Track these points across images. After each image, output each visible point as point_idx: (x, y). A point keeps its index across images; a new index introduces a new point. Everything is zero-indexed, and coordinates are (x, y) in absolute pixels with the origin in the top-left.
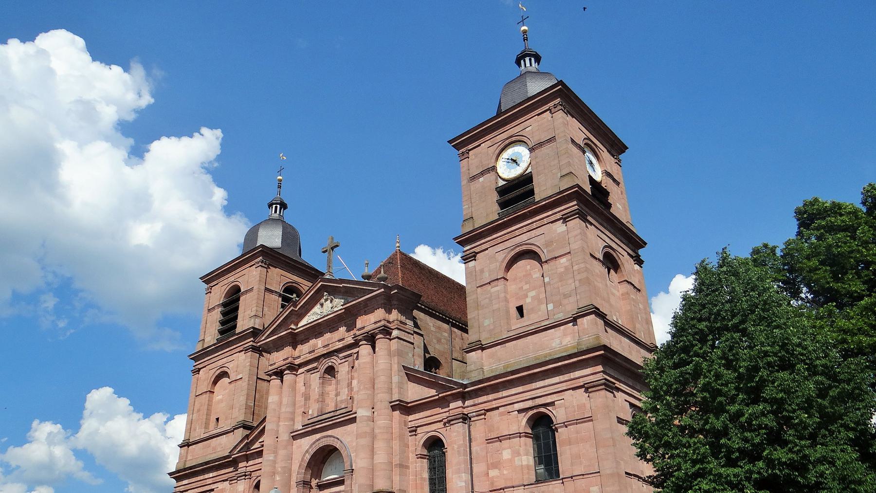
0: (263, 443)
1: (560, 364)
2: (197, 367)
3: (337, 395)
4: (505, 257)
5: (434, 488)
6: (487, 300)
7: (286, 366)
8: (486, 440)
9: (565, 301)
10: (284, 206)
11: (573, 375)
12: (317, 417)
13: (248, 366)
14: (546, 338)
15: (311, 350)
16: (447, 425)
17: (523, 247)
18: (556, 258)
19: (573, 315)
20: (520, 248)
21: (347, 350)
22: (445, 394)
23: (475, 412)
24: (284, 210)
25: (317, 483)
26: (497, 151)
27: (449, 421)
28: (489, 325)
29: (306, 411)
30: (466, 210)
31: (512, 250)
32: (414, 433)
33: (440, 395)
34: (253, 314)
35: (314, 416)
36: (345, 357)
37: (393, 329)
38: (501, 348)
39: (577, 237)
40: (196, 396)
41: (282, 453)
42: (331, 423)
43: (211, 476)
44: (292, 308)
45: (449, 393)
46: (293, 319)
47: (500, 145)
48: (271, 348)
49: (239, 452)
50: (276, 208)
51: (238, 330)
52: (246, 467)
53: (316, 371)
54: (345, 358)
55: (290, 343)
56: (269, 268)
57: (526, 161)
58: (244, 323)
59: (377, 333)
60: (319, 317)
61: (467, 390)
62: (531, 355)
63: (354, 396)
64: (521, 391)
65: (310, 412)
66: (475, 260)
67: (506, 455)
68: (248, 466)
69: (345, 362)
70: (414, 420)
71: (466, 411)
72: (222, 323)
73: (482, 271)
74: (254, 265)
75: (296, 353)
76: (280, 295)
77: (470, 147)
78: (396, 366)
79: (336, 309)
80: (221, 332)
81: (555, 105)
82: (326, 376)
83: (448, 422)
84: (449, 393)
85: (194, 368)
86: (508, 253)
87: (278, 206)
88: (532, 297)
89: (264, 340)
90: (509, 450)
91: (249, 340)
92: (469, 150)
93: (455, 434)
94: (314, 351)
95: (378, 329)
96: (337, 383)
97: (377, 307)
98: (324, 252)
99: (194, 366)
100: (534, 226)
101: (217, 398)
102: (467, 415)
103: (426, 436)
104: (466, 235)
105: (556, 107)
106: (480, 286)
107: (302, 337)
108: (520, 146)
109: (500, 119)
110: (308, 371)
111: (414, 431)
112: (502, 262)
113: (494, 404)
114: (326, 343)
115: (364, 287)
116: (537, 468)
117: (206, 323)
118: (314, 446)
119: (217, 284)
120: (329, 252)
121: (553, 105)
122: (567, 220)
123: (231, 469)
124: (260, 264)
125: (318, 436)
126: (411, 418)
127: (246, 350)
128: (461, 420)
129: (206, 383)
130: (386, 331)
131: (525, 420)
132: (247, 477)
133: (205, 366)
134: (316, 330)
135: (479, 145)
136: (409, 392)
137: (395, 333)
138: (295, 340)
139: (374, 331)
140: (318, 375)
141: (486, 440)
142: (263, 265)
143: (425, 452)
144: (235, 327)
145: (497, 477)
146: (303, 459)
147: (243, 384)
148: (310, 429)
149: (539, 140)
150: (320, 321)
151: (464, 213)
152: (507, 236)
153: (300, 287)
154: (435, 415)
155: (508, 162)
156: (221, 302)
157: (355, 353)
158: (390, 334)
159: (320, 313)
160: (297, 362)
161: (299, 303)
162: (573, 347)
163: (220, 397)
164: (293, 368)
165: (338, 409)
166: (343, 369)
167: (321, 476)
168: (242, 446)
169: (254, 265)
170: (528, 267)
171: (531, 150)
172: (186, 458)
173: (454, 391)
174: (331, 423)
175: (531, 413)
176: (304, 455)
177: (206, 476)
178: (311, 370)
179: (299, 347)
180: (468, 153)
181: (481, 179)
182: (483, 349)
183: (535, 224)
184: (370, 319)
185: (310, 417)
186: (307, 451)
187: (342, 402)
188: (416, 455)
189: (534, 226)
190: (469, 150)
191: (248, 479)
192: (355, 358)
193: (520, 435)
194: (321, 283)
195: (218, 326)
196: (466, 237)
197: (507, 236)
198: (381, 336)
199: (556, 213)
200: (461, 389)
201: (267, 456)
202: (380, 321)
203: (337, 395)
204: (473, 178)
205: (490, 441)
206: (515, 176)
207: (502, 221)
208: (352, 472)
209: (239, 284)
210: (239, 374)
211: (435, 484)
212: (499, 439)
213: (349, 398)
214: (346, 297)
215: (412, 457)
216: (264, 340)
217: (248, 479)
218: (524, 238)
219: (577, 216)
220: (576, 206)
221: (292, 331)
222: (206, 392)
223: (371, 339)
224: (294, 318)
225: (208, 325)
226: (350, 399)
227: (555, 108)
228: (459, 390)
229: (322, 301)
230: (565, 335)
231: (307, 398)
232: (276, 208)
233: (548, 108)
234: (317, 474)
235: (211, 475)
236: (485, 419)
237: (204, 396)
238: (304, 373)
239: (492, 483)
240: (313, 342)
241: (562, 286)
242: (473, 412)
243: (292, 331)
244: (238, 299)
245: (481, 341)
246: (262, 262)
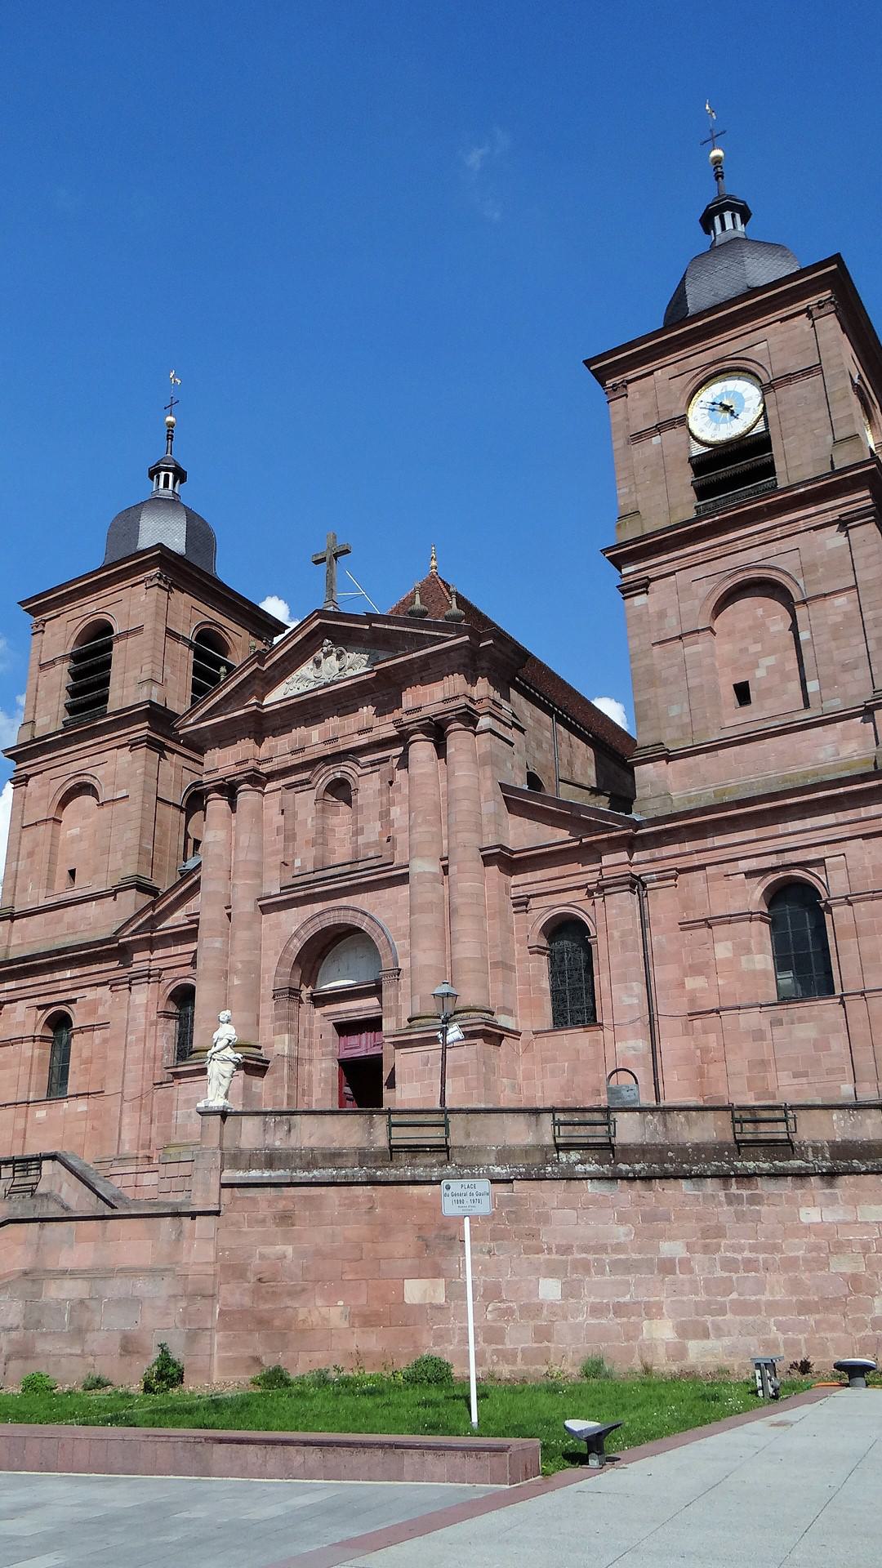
0: (198, 917)
1: (842, 790)
2: (23, 772)
3: (358, 832)
4: (713, 590)
5: (562, 1007)
6: (676, 669)
7: (245, 775)
8: (680, 924)
9: (847, 677)
10: (180, 475)
11: (863, 812)
12: (314, 872)
13: (140, 774)
14: (804, 744)
15: (297, 746)
16: (596, 895)
17: (752, 572)
18: (825, 595)
19: (865, 702)
20: (746, 574)
21: (376, 750)
22: (594, 838)
23: (656, 873)
24: (181, 483)
25: (311, 994)
26: (691, 388)
27: (601, 889)
28: (680, 716)
29: (286, 861)
30: (625, 498)
31: (729, 577)
32: (524, 907)
33: (584, 840)
34: (145, 676)
35: (308, 871)
36: (373, 763)
37: (480, 715)
38: (707, 758)
39: (871, 559)
40: (23, 827)
41: (242, 935)
42: (348, 883)
43: (68, 976)
44: (256, 665)
45: (605, 836)
46: (255, 687)
47: (697, 375)
48: (207, 740)
49: (134, 933)
50: (167, 477)
51: (113, 705)
52: (150, 961)
53: (306, 787)
54: (371, 766)
55: (250, 732)
56: (172, 592)
57: (752, 410)
58: (123, 692)
59: (452, 719)
60: (312, 686)
61: (640, 832)
62: (773, 774)
63: (397, 836)
64: (754, 837)
65: (298, 863)
66: (647, 593)
67: (723, 951)
68: (153, 960)
69: (371, 773)
70: (522, 885)
71: (634, 870)
72: (73, 692)
73: (662, 615)
74: (142, 582)
75: (263, 751)
76: (191, 646)
77: (630, 375)
78: (489, 783)
79: (350, 673)
80: (72, 709)
81: (820, 302)
82: (329, 797)
83: (601, 889)
84: (605, 836)
85: (14, 775)
86: (720, 584)
87: (171, 474)
88: (767, 667)
90: (729, 944)
91: (139, 726)
92: (629, 382)
93: (614, 911)
94: (302, 750)
95: (454, 713)
96: (357, 811)
97: (447, 671)
98: (317, 562)
99: (15, 771)
100: (778, 533)
101: (68, 832)
102: (638, 878)
103: (549, 913)
104: (631, 544)
105: (823, 307)
106: (659, 643)
107: (278, 722)
108: (739, 379)
109: (700, 323)
110: (289, 787)
111: (522, 904)
112: (708, 598)
113: (696, 860)
114: (331, 736)
115: (424, 632)
116: (779, 977)
117: (37, 691)
118: (309, 925)
119: (58, 616)
120: (330, 563)
121: (817, 301)
122: (849, 525)
123: (115, 964)
124: (156, 581)
125: (318, 907)
126: (515, 880)
127: (133, 745)
128: (628, 887)
129: (44, 804)
130: (469, 718)
131: (760, 891)
132: (151, 980)
133: (41, 772)
134: (309, 710)
135: (651, 373)
136: (511, 833)
137: (484, 722)
138: (261, 726)
139: (446, 715)
140: (312, 795)
141: (680, 924)
142: (162, 584)
143: (544, 943)
144: (104, 699)
145: (703, 990)
146: (286, 949)
147: (133, 809)
148: (302, 893)
149: (784, 370)
150: (320, 692)
151: (621, 502)
152: (718, 552)
153: (223, 634)
154: (568, 876)
155: (713, 410)
156: (69, 651)
157: (394, 757)
158: (475, 723)
159: (313, 678)
160: (265, 768)
161: (271, 657)
162: (865, 762)
163: (76, 831)
164: (257, 780)
165: (359, 859)
166: (368, 786)
167: (316, 980)
168: (141, 921)
169: (142, 582)
170: (760, 612)
171: (766, 388)
172: (9, 941)
173: (614, 834)
174: (348, 883)
175: (772, 878)
176: (290, 941)
177: (58, 975)
178: (297, 786)
179: (269, 742)
180: (625, 387)
181: (656, 440)
182: (669, 759)
183: (778, 529)
184: (432, 695)
185: (296, 873)
186: (295, 935)
187: (368, 845)
188: (529, 948)
189: (778, 533)
190: (629, 382)
191: (152, 982)
192: (394, 767)
193: (749, 916)
194: (319, 621)
195: (64, 698)
196: (630, 547)
197: (718, 552)
198: (459, 725)
199: (825, 511)
200: (631, 831)
201: (209, 943)
202: (456, 698)
203: (358, 832)
204: (638, 437)
205: (686, 926)
206: (730, 436)
207: (711, 520)
208: (398, 975)
209: (108, 618)
211: (564, 1001)
212: (708, 923)
213: (386, 839)
214: (373, 651)
215: (519, 950)
217: (152, 982)
218: (754, 555)
219: (873, 518)
220: (870, 500)
221: (259, 709)
222: (46, 820)
223: (437, 732)
224: (257, 686)
225: (41, 694)
226: (388, 841)
227: (820, 308)
228: (625, 832)
229: (319, 655)
230: (846, 738)
231: (290, 837)
232: (167, 477)
233: (805, 306)
234: (310, 978)
235: (68, 974)
236: (676, 886)
237: (42, 827)
238: (280, 789)
239: (692, 1001)
240: (299, 732)
241: (838, 648)
242: (652, 873)
243: (259, 709)
244: (109, 647)
245: (662, 744)
246: (159, 578)
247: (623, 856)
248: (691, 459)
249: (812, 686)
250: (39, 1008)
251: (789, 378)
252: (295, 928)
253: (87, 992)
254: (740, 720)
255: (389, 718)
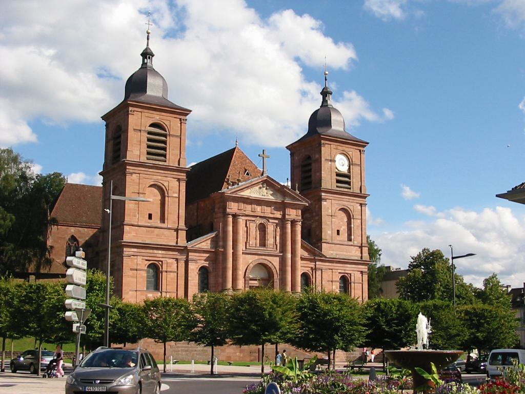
36: (272, 223)
65: (251, 243)
89: (230, 193)
100: (351, 201)
125: (257, 257)
175: (342, 275)
187: (270, 244)
210: (174, 193)
216: (230, 193)
218: (346, 203)
247: (320, 263)
248: (336, 172)
249: (353, 237)
250: (146, 260)
251: (356, 164)
252: (251, 261)
253: (167, 259)
254: (338, 239)
255: (279, 213)
